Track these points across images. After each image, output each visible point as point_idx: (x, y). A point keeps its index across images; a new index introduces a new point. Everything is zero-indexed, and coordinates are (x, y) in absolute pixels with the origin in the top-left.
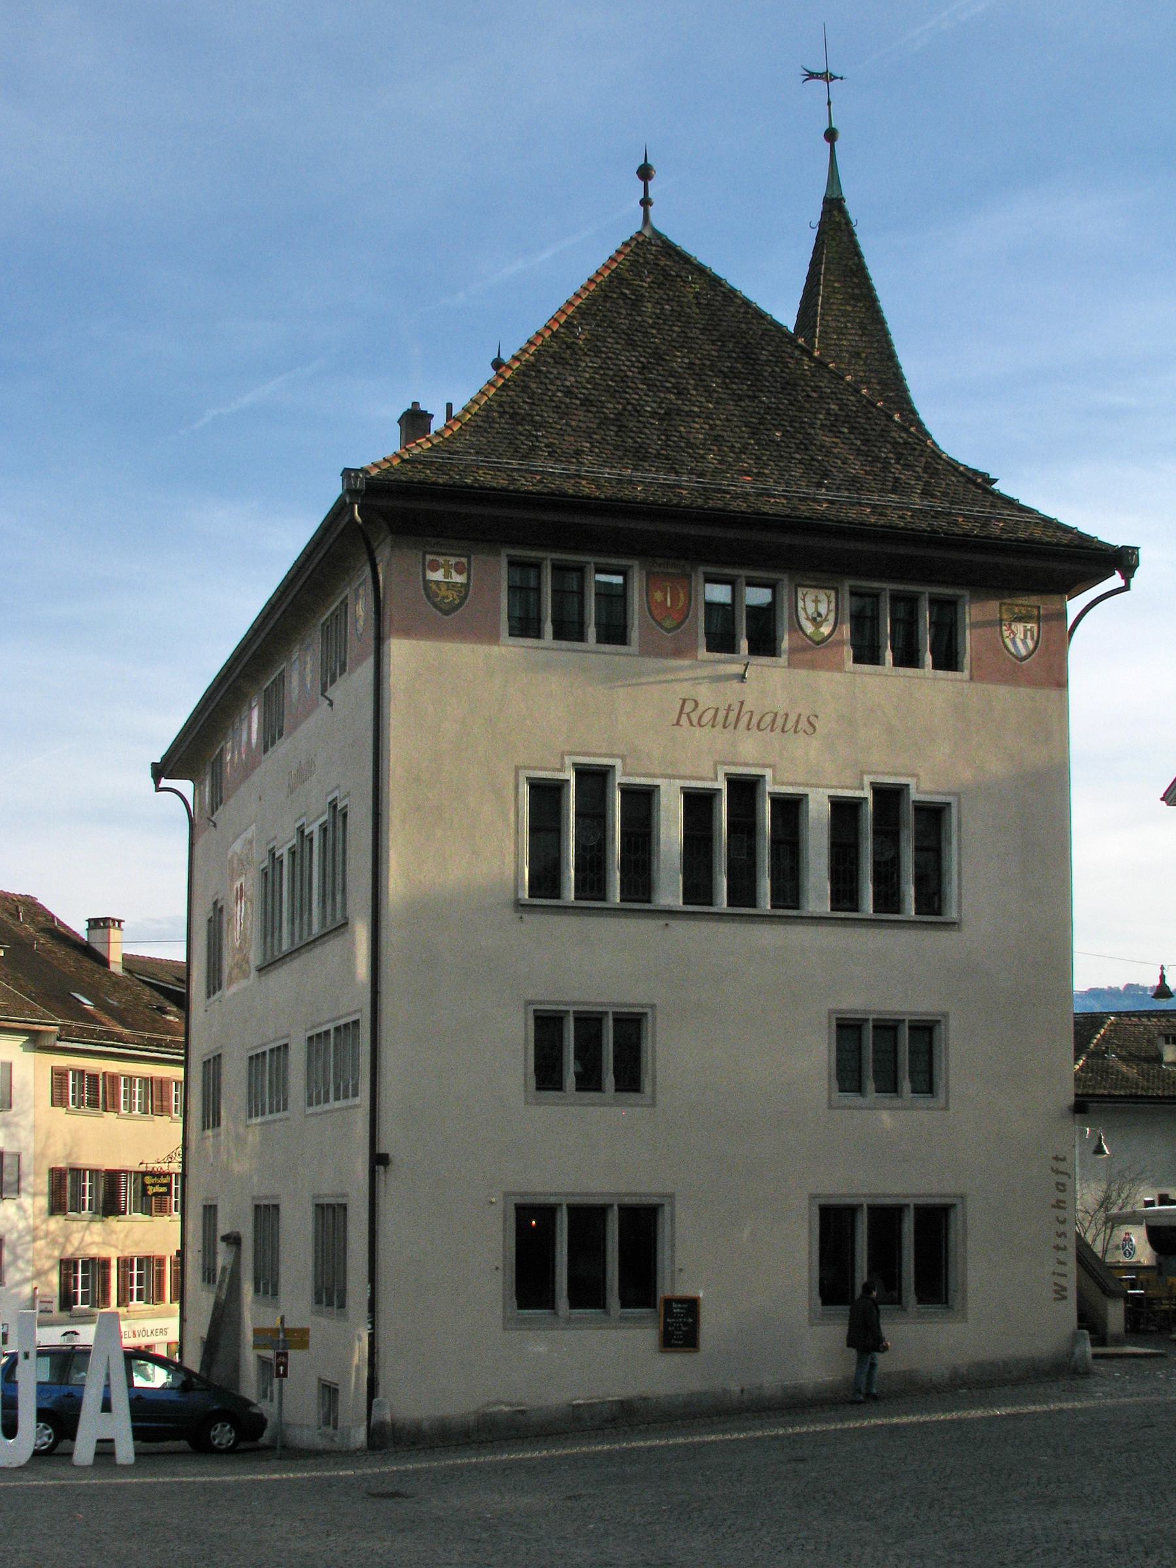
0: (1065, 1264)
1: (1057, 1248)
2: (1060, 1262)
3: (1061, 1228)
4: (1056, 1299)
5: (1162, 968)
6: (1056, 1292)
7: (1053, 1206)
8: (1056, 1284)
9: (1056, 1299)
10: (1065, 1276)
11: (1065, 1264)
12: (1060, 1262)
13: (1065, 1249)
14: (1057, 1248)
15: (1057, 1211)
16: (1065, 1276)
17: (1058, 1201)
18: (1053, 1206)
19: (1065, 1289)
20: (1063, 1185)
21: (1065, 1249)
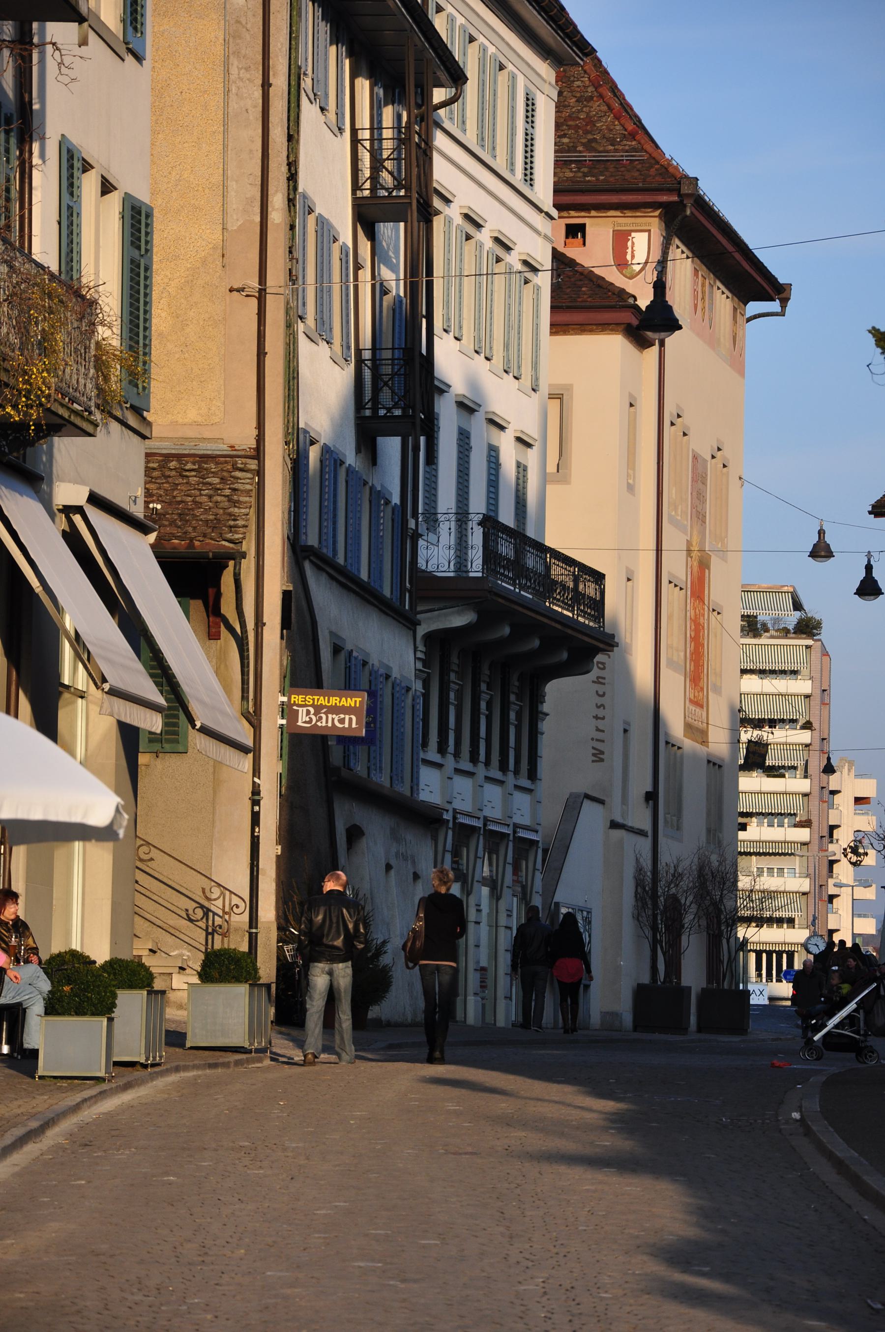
0: (603, 731)
1: (596, 717)
2: (598, 730)
3: (600, 700)
4: (593, 761)
5: (231, 290)
6: (594, 755)
7: (593, 682)
8: (593, 748)
9: (593, 761)
10: (603, 741)
11: (603, 731)
12: (598, 730)
13: (603, 718)
14: (596, 717)
15: (597, 687)
16: (603, 741)
17: (598, 678)
18: (593, 682)
19: (602, 753)
20: (603, 664)
21: (603, 718)
